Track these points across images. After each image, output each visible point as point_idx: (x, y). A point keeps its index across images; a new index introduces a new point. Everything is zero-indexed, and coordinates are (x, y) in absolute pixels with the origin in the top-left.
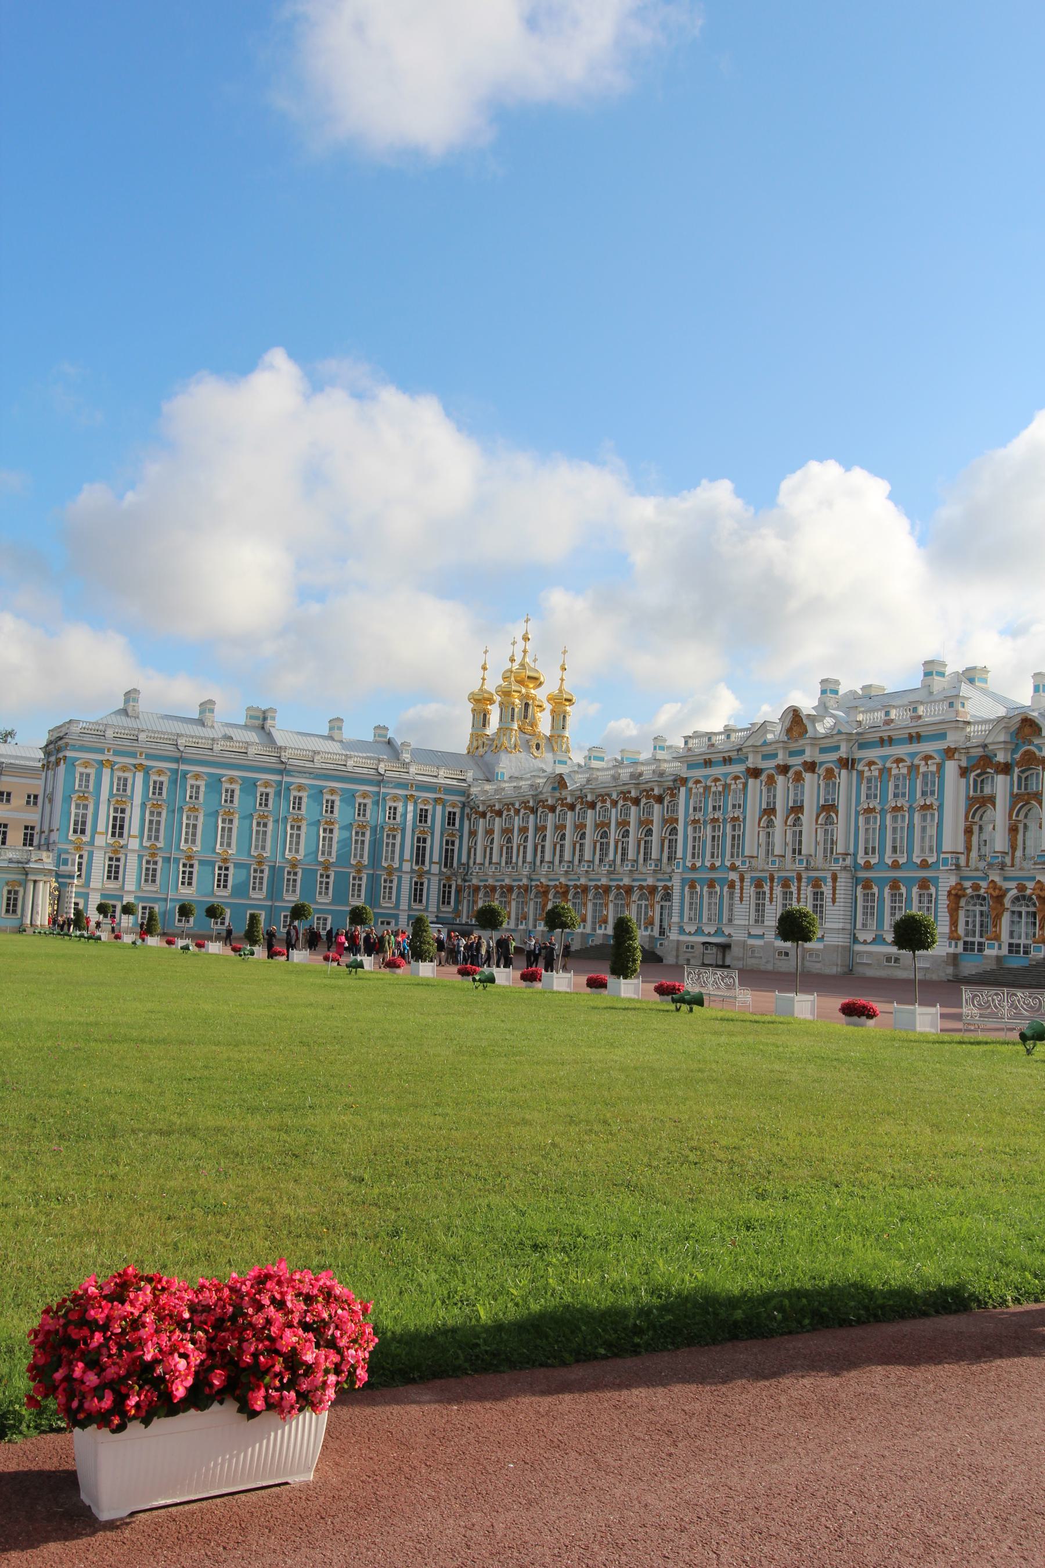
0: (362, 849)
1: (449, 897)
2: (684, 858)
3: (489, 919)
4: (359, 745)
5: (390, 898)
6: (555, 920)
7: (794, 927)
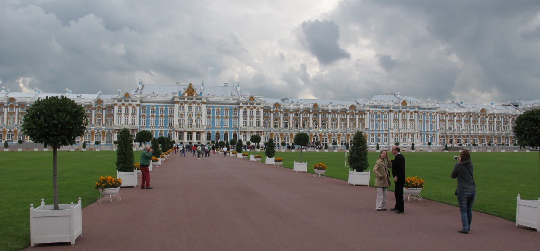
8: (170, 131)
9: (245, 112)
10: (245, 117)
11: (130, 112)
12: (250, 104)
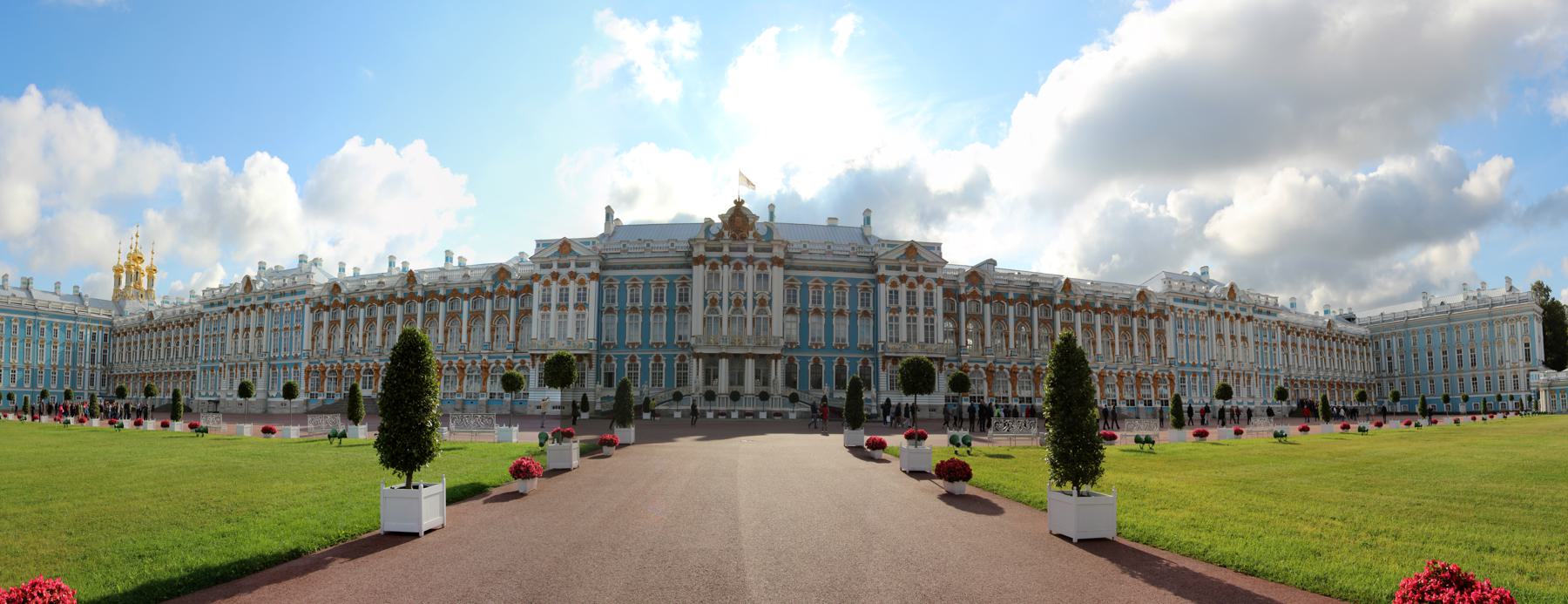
3: (121, 393)
4: (66, 297)
6: (148, 392)
7: (245, 391)
8: (682, 358)
9: (894, 296)
10: (892, 311)
11: (572, 300)
12: (909, 269)
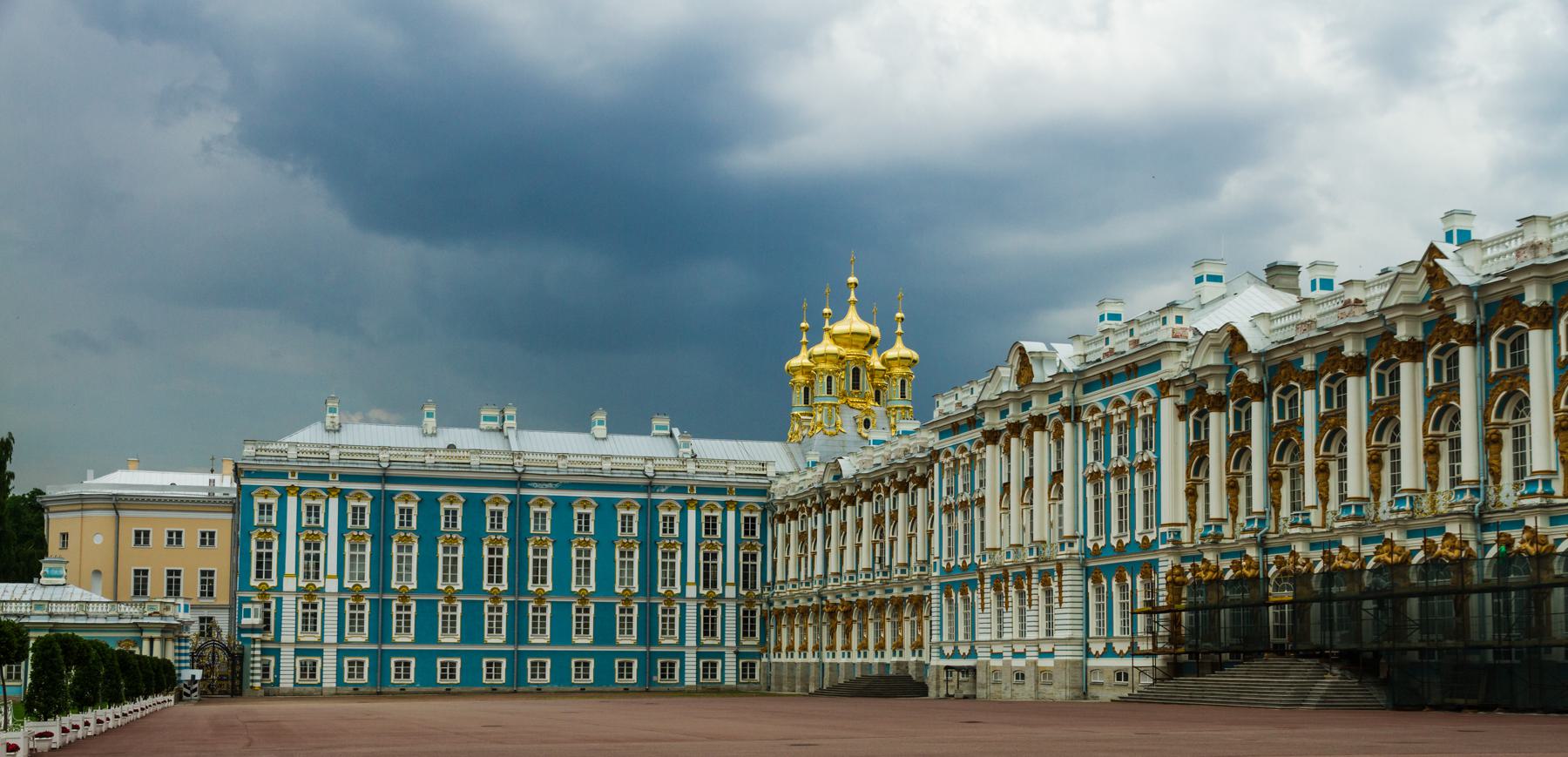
0: (630, 573)
1: (753, 627)
2: (940, 557)
5: (672, 633)
